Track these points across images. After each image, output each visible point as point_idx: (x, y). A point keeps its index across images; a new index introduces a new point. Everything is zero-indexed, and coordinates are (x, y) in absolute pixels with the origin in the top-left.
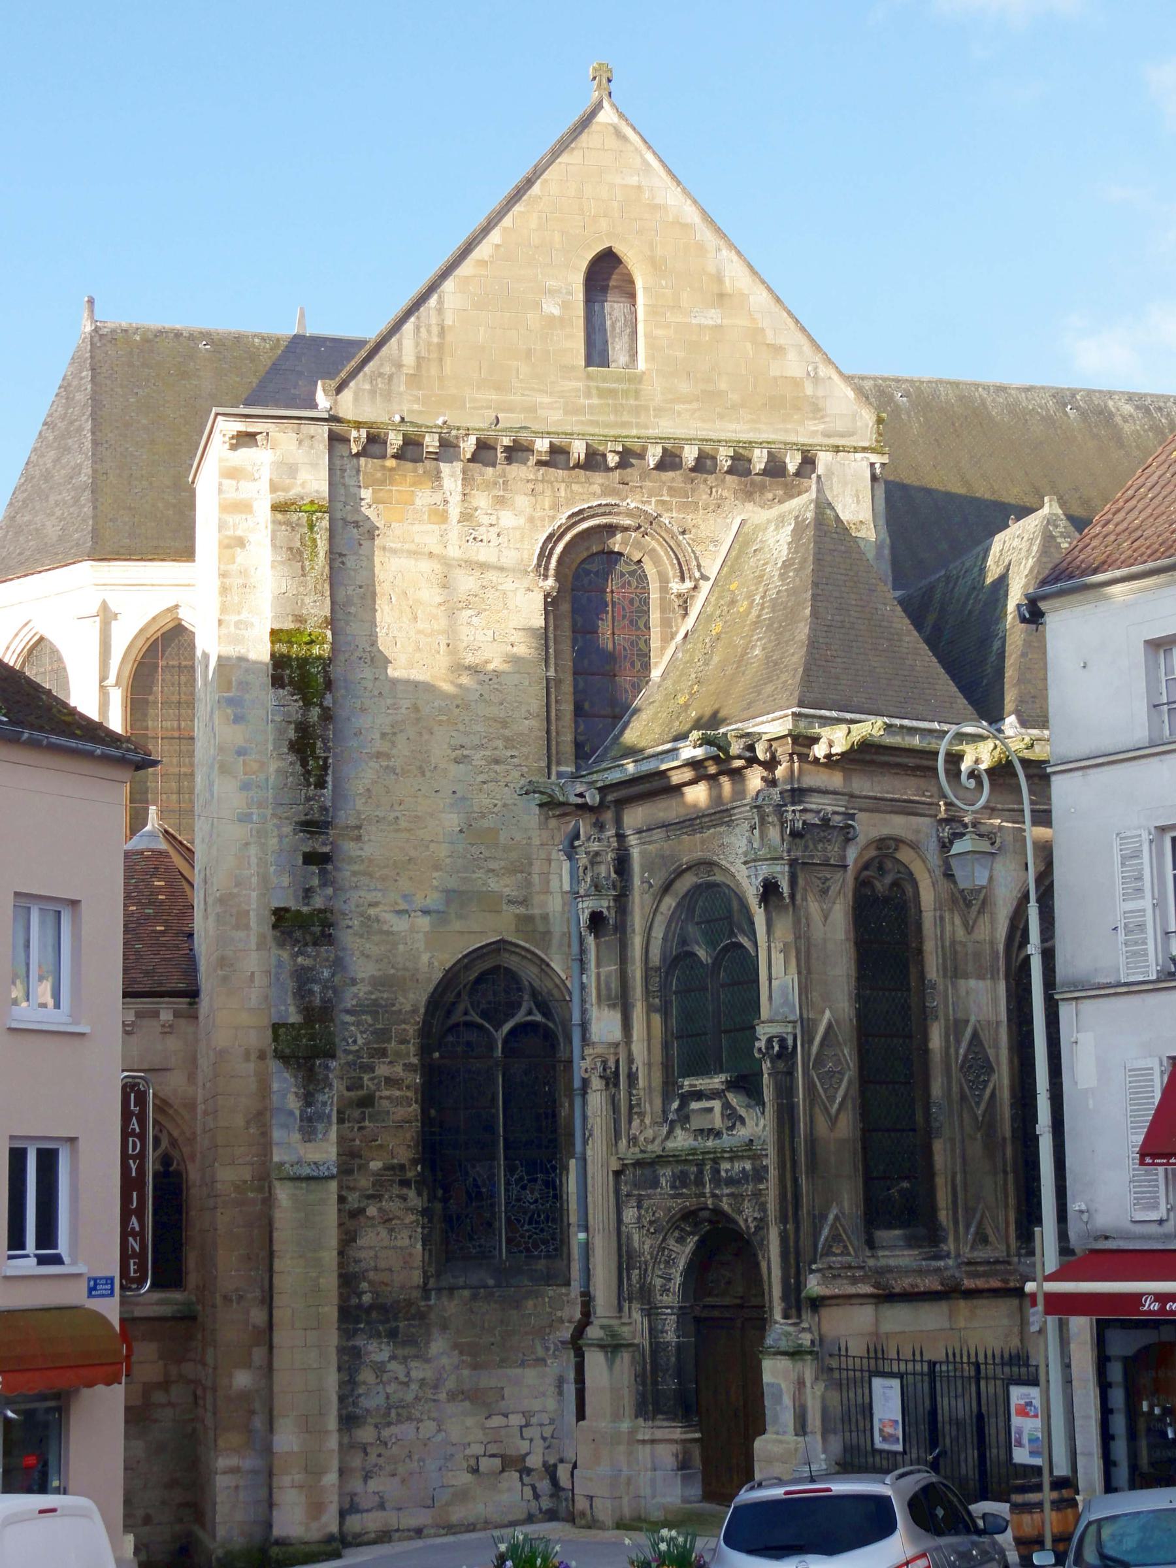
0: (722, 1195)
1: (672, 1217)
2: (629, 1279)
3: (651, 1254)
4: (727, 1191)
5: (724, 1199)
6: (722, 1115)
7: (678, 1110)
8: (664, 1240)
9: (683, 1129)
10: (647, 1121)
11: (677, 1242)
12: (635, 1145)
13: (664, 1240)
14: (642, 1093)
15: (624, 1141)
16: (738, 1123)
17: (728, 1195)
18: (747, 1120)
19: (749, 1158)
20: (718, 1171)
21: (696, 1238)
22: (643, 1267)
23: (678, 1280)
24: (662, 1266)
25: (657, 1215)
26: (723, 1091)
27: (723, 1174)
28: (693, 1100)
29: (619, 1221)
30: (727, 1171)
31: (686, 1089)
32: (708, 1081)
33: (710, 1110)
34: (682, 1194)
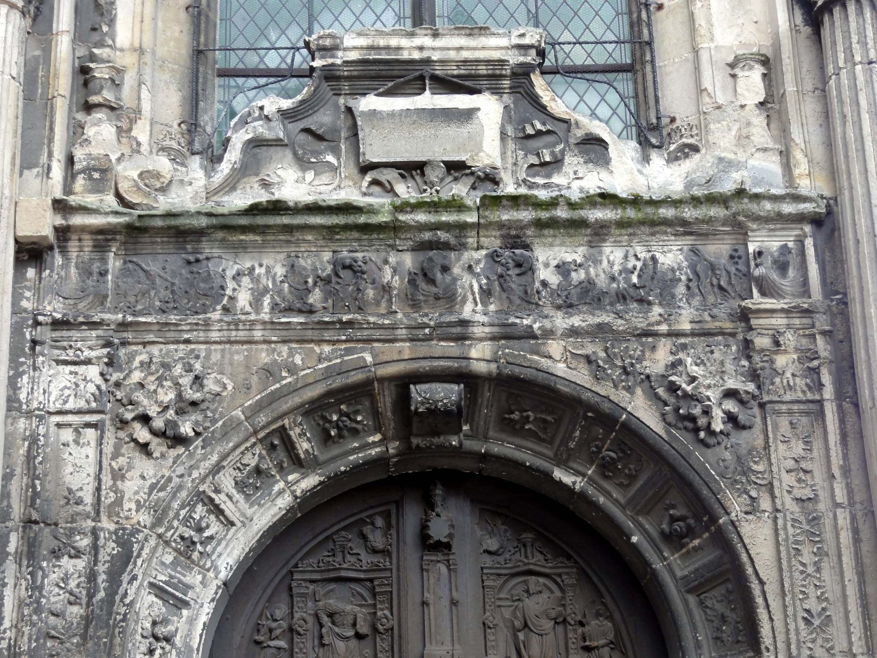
0: (548, 334)
1: (274, 398)
2: (36, 588)
3: (160, 515)
4: (561, 321)
5: (555, 347)
6: (503, 135)
7: (287, 115)
8: (217, 469)
9: (303, 163)
10: (142, 132)
11: (240, 485)
12: (97, 187)
13: (217, 469)
14: (127, 60)
15: (57, 172)
16: (572, 161)
17: (573, 332)
18: (612, 151)
19: (684, 228)
20: (526, 268)
21: (310, 482)
22: (110, 548)
23: (205, 613)
24: (169, 559)
25: (211, 385)
26: (522, 73)
27: (546, 274)
28: (365, 94)
29: (13, 403)
30: (563, 269)
31: (353, 56)
32: (462, 41)
33: (468, 115)
34: (350, 324)
